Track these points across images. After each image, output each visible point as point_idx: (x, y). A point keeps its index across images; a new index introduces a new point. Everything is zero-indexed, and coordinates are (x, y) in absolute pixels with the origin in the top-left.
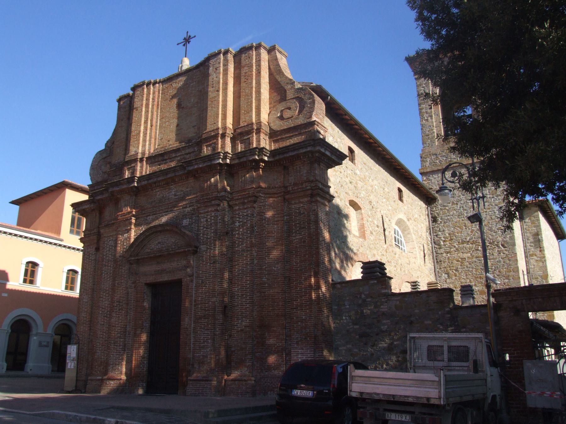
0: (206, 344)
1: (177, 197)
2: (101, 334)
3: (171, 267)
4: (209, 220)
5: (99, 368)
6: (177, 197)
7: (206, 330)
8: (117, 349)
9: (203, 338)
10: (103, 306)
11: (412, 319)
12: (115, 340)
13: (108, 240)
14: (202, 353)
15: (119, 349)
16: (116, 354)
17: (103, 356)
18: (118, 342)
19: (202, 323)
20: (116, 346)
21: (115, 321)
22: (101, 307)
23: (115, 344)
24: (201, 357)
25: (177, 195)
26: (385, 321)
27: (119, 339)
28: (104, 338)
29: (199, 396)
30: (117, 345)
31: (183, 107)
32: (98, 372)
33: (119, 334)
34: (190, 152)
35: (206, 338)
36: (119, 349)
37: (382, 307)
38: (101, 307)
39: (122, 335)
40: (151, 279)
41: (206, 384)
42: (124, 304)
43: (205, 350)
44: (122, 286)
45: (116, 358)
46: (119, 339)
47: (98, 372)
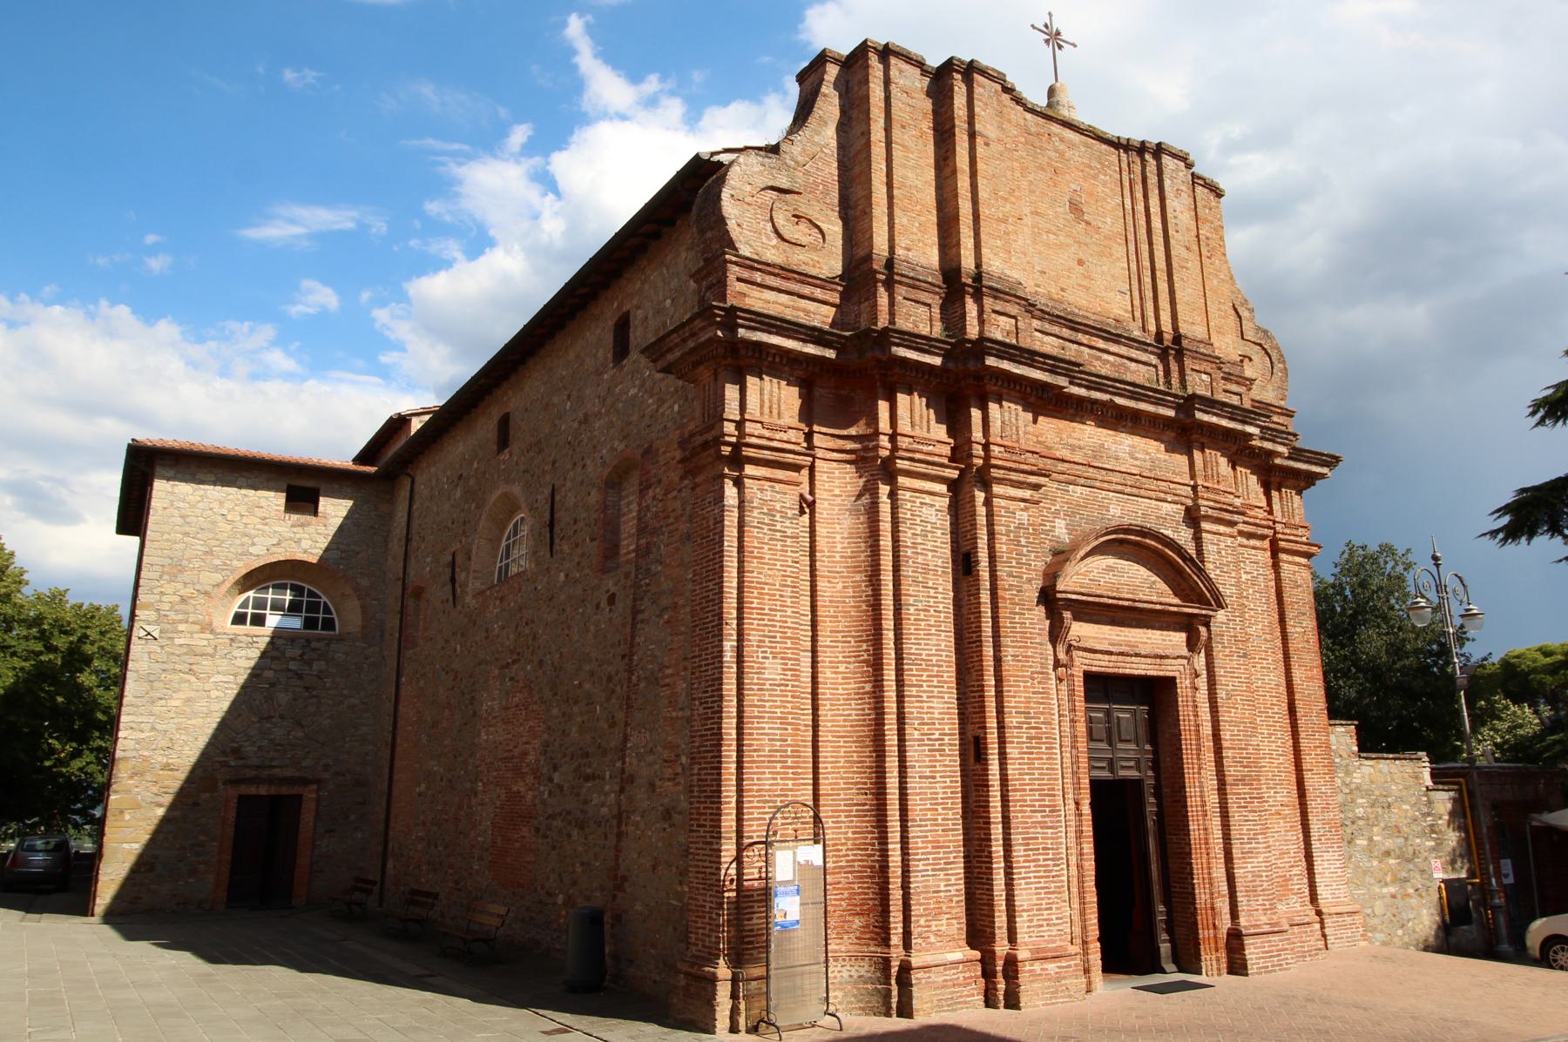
0: (1253, 845)
1: (1138, 463)
2: (929, 810)
3: (1149, 641)
4: (1223, 552)
5: (934, 923)
6: (1138, 463)
7: (1249, 811)
8: (1039, 860)
9: (1248, 830)
10: (925, 716)
11: (1389, 799)
12: (1028, 833)
13: (918, 501)
14: (1249, 865)
15: (1045, 860)
16: (1035, 877)
17: (943, 884)
18: (1037, 838)
19: (1239, 794)
20: (1032, 850)
21: (1020, 774)
22: (917, 718)
23: (1028, 844)
24: (1250, 878)
25: (1136, 459)
26: (1360, 801)
27: (1039, 830)
28: (940, 821)
29: (1275, 971)
30: (1038, 849)
31: (1088, 223)
32: (933, 939)
33: (1039, 815)
34: (1140, 358)
35: (1252, 830)
36: (1045, 860)
37: (1355, 775)
38: (917, 718)
39: (1048, 816)
40: (1102, 664)
41: (1281, 941)
42: (1043, 723)
43: (1255, 860)
44: (1031, 667)
45: (1036, 888)
46: (1039, 830)
47: (933, 939)
